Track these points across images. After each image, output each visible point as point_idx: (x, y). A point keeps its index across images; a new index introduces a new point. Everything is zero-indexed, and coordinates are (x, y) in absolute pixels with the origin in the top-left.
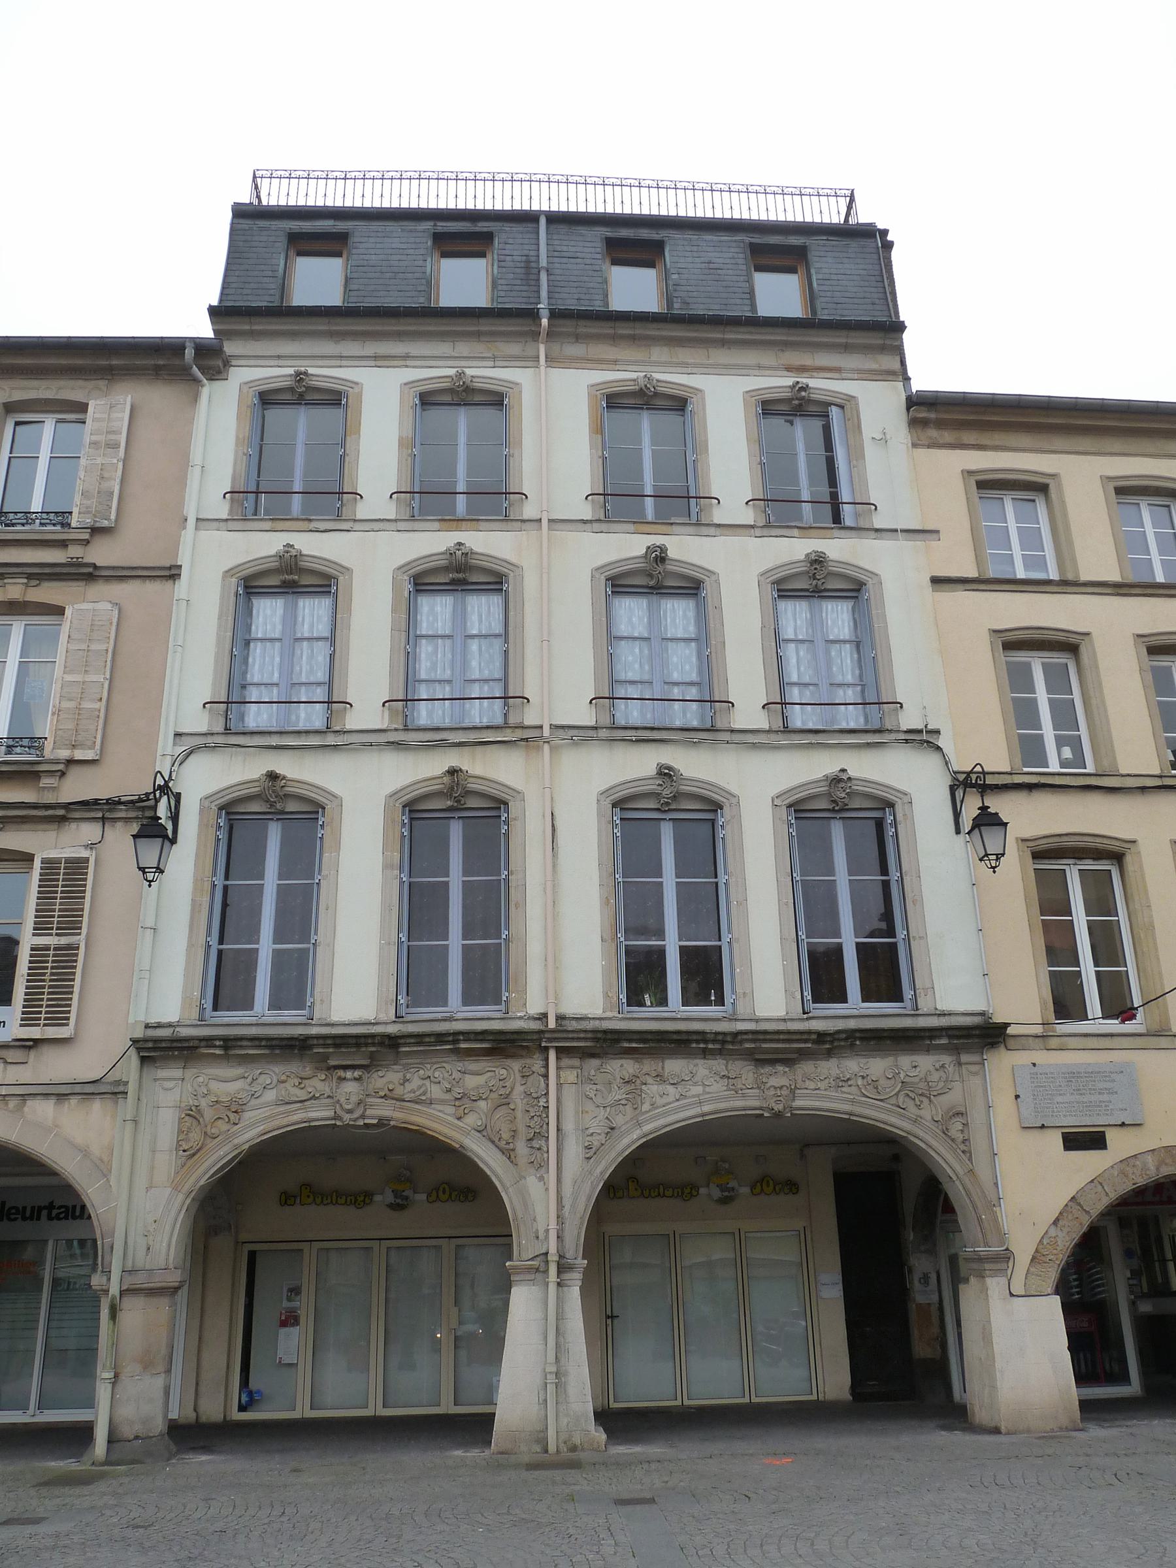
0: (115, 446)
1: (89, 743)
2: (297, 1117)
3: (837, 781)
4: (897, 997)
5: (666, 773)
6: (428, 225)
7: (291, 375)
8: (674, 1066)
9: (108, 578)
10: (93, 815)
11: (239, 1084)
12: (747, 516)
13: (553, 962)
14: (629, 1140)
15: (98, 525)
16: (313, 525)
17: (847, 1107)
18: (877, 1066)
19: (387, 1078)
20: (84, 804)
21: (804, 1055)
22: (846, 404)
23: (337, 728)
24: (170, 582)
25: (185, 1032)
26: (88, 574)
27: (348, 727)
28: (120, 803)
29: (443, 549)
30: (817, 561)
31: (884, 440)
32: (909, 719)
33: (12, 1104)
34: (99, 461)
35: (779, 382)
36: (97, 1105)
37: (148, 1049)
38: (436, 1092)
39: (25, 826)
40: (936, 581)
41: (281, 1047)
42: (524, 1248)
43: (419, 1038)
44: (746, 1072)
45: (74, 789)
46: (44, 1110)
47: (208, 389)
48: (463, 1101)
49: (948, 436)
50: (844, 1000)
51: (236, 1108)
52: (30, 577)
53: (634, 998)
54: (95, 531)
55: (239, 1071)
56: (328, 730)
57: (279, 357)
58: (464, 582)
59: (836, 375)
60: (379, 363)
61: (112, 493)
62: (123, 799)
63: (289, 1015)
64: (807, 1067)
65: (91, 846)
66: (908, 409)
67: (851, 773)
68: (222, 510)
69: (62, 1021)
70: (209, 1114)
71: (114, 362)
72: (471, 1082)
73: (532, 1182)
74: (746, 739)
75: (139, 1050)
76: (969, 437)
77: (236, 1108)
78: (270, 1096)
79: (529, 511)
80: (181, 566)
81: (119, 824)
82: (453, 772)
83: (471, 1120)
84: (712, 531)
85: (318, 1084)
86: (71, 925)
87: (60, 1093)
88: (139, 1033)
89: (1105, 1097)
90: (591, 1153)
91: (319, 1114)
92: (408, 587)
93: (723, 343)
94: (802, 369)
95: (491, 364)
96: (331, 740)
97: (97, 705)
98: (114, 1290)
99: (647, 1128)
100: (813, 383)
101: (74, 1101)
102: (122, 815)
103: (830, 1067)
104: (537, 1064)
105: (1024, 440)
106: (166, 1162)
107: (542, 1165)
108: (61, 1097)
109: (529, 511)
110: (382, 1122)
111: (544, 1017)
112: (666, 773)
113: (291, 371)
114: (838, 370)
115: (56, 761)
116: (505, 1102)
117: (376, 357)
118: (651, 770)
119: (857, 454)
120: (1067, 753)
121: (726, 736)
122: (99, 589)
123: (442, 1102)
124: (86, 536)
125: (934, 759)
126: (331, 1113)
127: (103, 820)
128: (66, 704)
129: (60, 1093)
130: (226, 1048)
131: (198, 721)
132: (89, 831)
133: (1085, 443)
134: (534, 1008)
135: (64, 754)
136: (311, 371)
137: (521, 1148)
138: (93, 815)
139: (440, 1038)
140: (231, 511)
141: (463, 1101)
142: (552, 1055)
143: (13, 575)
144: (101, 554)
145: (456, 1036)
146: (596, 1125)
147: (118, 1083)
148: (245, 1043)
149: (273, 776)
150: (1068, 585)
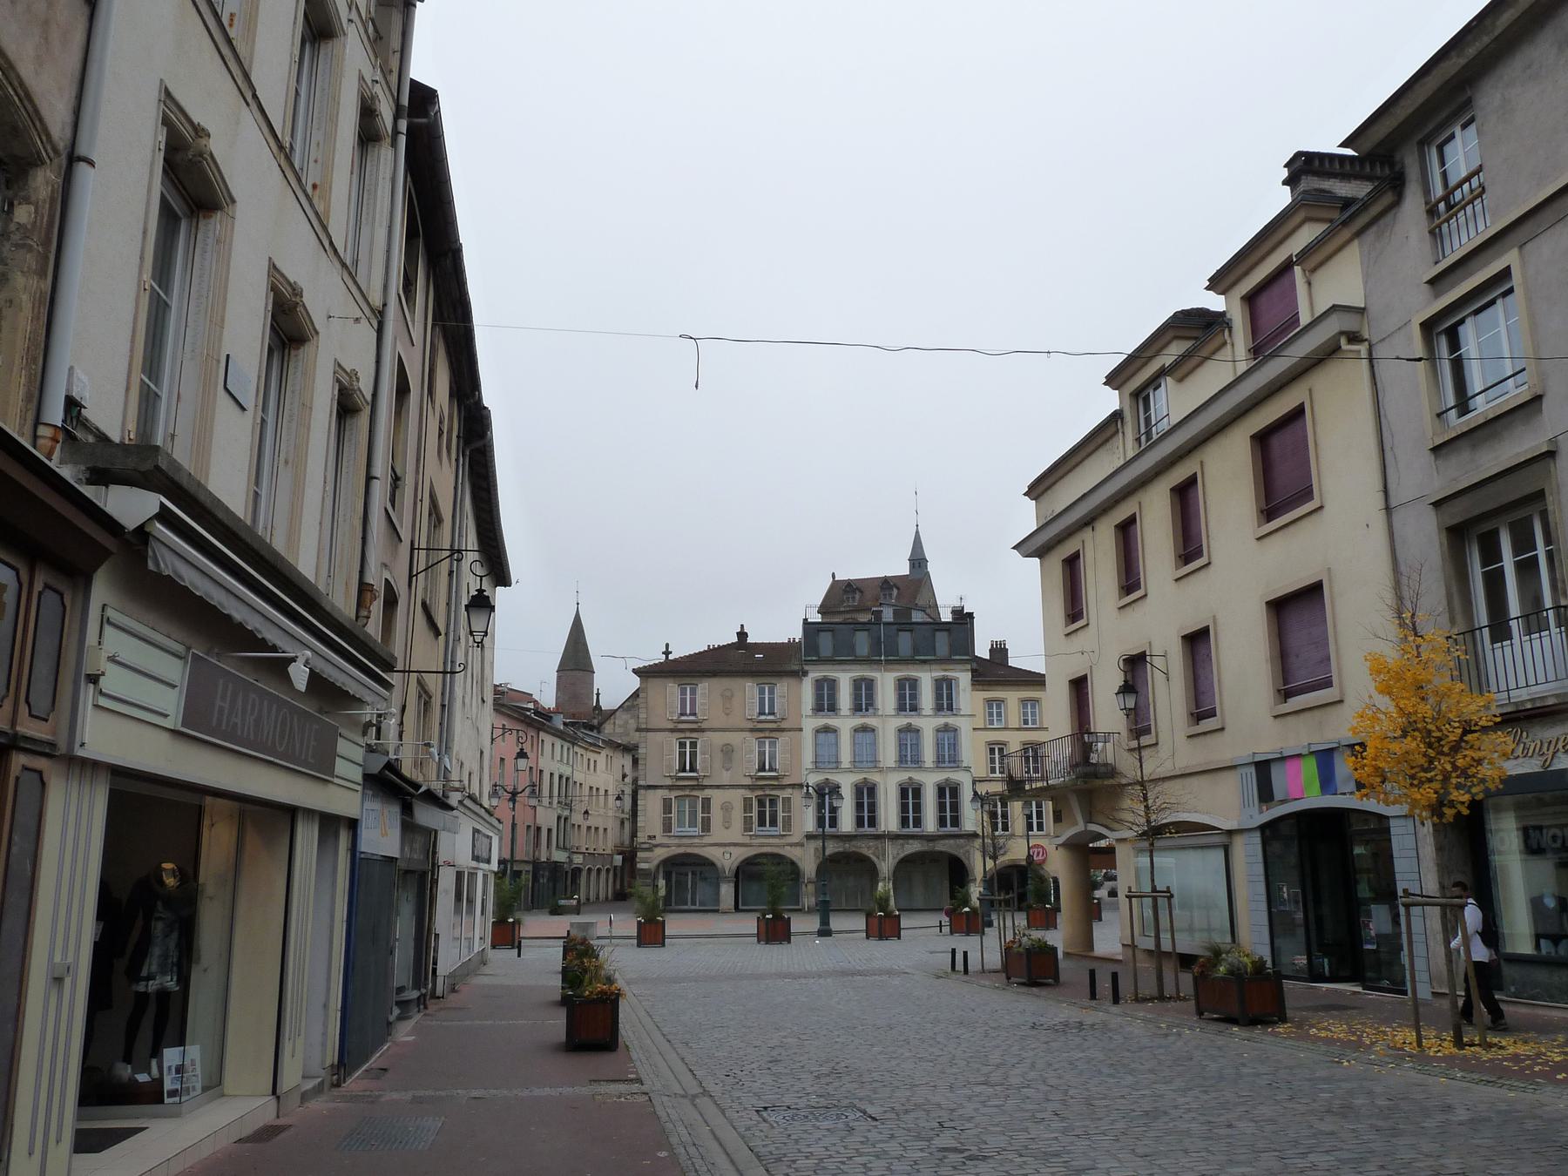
2: (837, 850)
3: (947, 780)
4: (958, 827)
5: (910, 778)
8: (911, 841)
12: (930, 712)
13: (886, 820)
14: (902, 855)
18: (952, 841)
19: (854, 843)
21: (936, 840)
22: (956, 679)
26: (783, 730)
30: (946, 725)
31: (964, 690)
32: (965, 764)
35: (939, 674)
36: (798, 848)
40: (974, 729)
42: (881, 876)
43: (861, 836)
44: (925, 843)
45: (786, 781)
47: (805, 679)
48: (869, 848)
49: (981, 687)
50: (946, 826)
53: (903, 827)
54: (783, 719)
56: (837, 768)
63: (833, 829)
64: (937, 842)
68: (810, 713)
73: (883, 864)
74: (927, 770)
76: (985, 688)
79: (880, 713)
82: (865, 778)
83: (870, 851)
85: (841, 844)
86: (790, 812)
87: (791, 845)
90: (894, 858)
91: (841, 850)
92: (853, 733)
94: (946, 670)
103: (942, 842)
104: (883, 841)
105: (1000, 688)
106: (813, 857)
107: (884, 860)
108: (791, 846)
109: (880, 713)
110: (853, 852)
112: (910, 778)
116: (877, 848)
119: (958, 693)
120: (1002, 770)
122: (785, 733)
129: (791, 845)
131: (810, 766)
132: (790, 791)
133: (1016, 688)
137: (881, 857)
139: (864, 835)
141: (869, 848)
144: (784, 725)
145: (867, 835)
146: (895, 852)
149: (827, 779)
150: (1005, 729)
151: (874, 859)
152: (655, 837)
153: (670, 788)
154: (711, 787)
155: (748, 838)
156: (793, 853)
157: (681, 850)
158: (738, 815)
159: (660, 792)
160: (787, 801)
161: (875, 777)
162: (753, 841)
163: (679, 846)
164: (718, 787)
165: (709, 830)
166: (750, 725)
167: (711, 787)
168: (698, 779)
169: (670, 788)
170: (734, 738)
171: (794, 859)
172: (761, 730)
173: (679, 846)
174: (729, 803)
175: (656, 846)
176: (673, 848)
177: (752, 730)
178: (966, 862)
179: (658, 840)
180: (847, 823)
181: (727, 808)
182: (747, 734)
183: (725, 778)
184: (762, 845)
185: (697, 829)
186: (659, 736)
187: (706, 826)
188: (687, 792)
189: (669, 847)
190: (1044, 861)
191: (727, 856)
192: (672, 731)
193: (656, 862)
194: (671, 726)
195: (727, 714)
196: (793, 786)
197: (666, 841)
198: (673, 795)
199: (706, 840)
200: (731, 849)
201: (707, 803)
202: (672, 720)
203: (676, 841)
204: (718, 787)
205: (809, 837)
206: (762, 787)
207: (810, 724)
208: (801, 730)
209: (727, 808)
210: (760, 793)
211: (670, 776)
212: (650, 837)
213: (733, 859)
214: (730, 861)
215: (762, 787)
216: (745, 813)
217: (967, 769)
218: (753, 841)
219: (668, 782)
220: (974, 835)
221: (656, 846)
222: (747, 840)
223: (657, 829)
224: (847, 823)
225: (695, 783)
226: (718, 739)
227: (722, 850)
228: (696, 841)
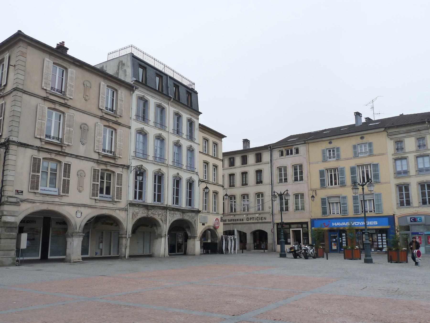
0: (123, 101)
1: (121, 155)
6: (155, 71)
7: (142, 95)
9: (121, 126)
10: (122, 167)
11: (138, 210)
15: (121, 116)
16: (145, 124)
17: (188, 219)
20: (121, 165)
23: (148, 159)
24: (129, 129)
25: (133, 202)
27: (149, 159)
28: (125, 165)
29: (158, 133)
32: (196, 171)
33: (114, 210)
34: (121, 103)
36: (123, 211)
37: (131, 205)
38: (156, 213)
39: (114, 167)
41: (144, 206)
45: (119, 162)
46: (118, 211)
51: (137, 213)
52: (113, 122)
55: (138, 208)
57: (141, 91)
58: (159, 138)
59: (194, 117)
60: (152, 97)
61: (123, 110)
62: (125, 165)
65: (123, 172)
66: (199, 126)
67: (192, 177)
69: (121, 199)
70: (135, 214)
71: (123, 84)
72: (160, 212)
73: (165, 226)
75: (129, 205)
76: (203, 131)
77: (137, 213)
78: (141, 212)
80: (131, 127)
81: (124, 169)
84: (182, 138)
86: (121, 185)
87: (120, 209)
88: (129, 202)
89: (205, 220)
92: (155, 138)
93: (185, 108)
95: (163, 102)
96: (147, 161)
97: (122, 148)
98: (128, 237)
99: (174, 220)
100: (193, 118)
101: (121, 211)
102: (125, 168)
106: (131, 220)
108: (120, 210)
111: (167, 205)
113: (143, 95)
114: (194, 117)
115: (118, 157)
117: (152, 96)
118: (176, 173)
121: (182, 169)
123: (157, 215)
124: (119, 117)
125: (197, 176)
126: (146, 215)
127: (123, 168)
128: (118, 147)
129: (120, 209)
130: (138, 205)
131: (133, 154)
132: (121, 169)
134: (166, 204)
135: (118, 156)
136: (145, 96)
138: (122, 167)
140: (135, 118)
141: (159, 215)
142: (168, 210)
143: (111, 121)
147: (126, 209)
148: (141, 205)
151: (160, 222)
152: (22, 192)
153: (39, 149)
154: (71, 155)
155: (94, 201)
156: (120, 216)
157: (44, 207)
158: (88, 182)
159: (30, 152)
160: (120, 176)
161: (164, 170)
162: (97, 204)
163: (43, 203)
164: (77, 157)
165: (68, 192)
166: (100, 114)
167: (71, 155)
168: (62, 147)
169: (39, 149)
170: (91, 121)
171: (121, 220)
172: (108, 120)
173: (43, 203)
174: (83, 171)
175: (23, 201)
176: (38, 204)
177: (102, 118)
178: (194, 226)
179: (26, 195)
180: (149, 198)
181: (81, 174)
182: (98, 120)
183: (81, 151)
184: (102, 208)
185: (56, 189)
186: (34, 101)
187: (66, 189)
188: (53, 156)
189: (34, 202)
190: (219, 226)
191: (79, 215)
192: (45, 99)
193: (21, 217)
194: (44, 94)
195: (86, 100)
196: (123, 166)
197: (31, 197)
198: (42, 155)
199: (65, 200)
200: (82, 209)
201: (68, 167)
202: (46, 90)
203: (41, 198)
204: (77, 157)
205: (132, 205)
206: (106, 163)
207: (136, 125)
208: (130, 128)
209: (81, 174)
210: (104, 167)
211: (40, 139)
212: (17, 191)
213: (83, 216)
214: (81, 219)
215: (106, 163)
216: (94, 181)
217: (197, 174)
218: (97, 204)
219: (38, 143)
220: (198, 212)
221: (23, 201)
222: (93, 203)
223: (24, 186)
224: (149, 198)
225: (59, 149)
226: (80, 118)
227: (75, 209)
228: (57, 200)
